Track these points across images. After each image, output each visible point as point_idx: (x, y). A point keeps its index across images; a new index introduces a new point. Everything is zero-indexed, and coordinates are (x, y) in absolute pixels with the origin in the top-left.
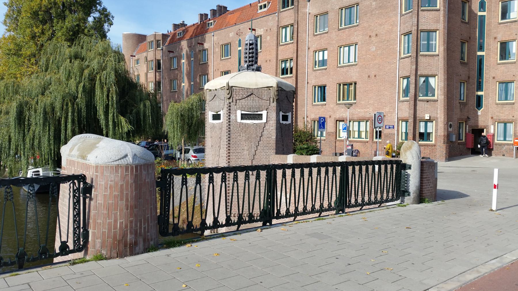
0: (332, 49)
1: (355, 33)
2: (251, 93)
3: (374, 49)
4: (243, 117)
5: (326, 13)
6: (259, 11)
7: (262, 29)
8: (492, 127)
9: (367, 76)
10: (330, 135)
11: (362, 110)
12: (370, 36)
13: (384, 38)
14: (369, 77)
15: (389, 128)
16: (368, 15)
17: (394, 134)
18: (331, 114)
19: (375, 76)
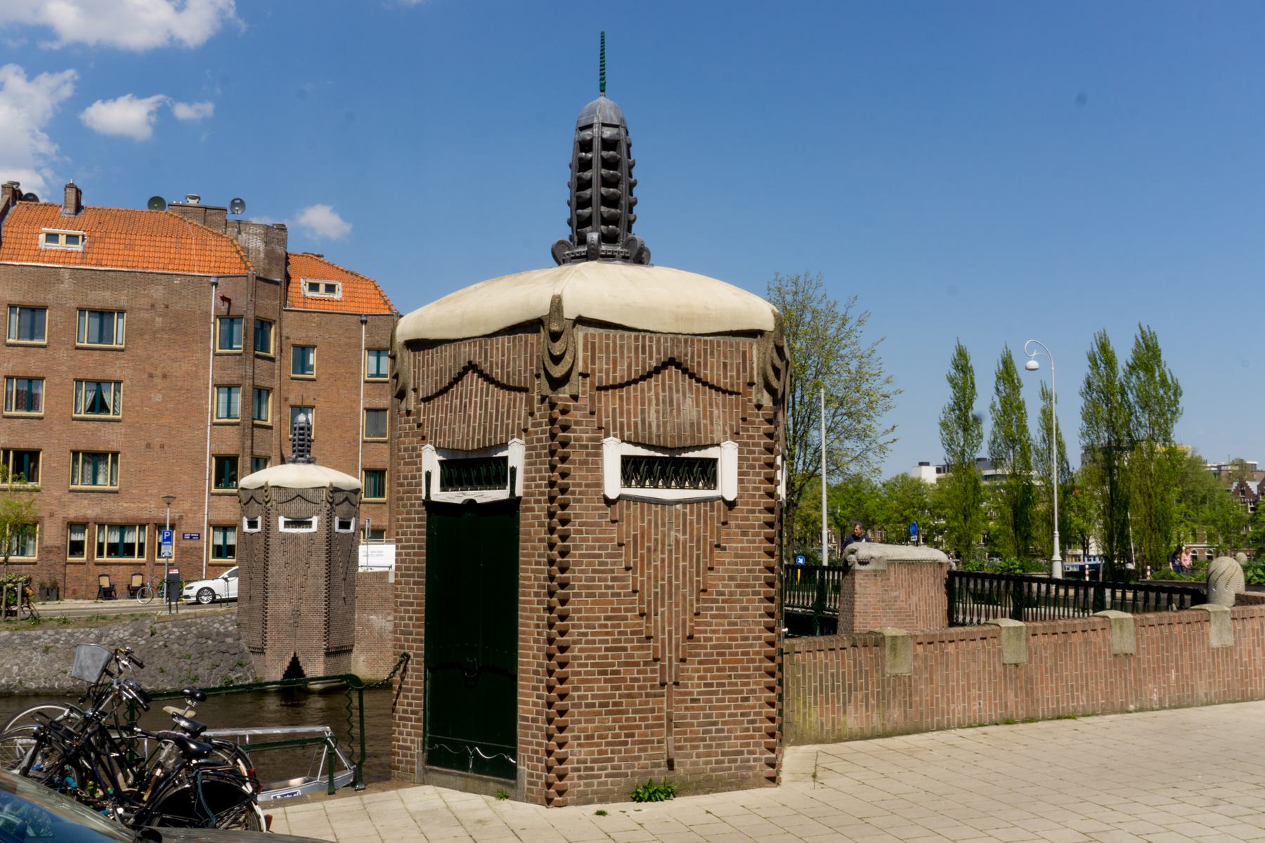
0: (57, 380)
1: (117, 362)
3: (158, 398)
5: (43, 309)
9: (144, 443)
10: (50, 552)
11: (132, 505)
13: (179, 384)
15: (191, 538)
16: (147, 337)
17: (202, 549)
18: (54, 508)
19: (162, 447)
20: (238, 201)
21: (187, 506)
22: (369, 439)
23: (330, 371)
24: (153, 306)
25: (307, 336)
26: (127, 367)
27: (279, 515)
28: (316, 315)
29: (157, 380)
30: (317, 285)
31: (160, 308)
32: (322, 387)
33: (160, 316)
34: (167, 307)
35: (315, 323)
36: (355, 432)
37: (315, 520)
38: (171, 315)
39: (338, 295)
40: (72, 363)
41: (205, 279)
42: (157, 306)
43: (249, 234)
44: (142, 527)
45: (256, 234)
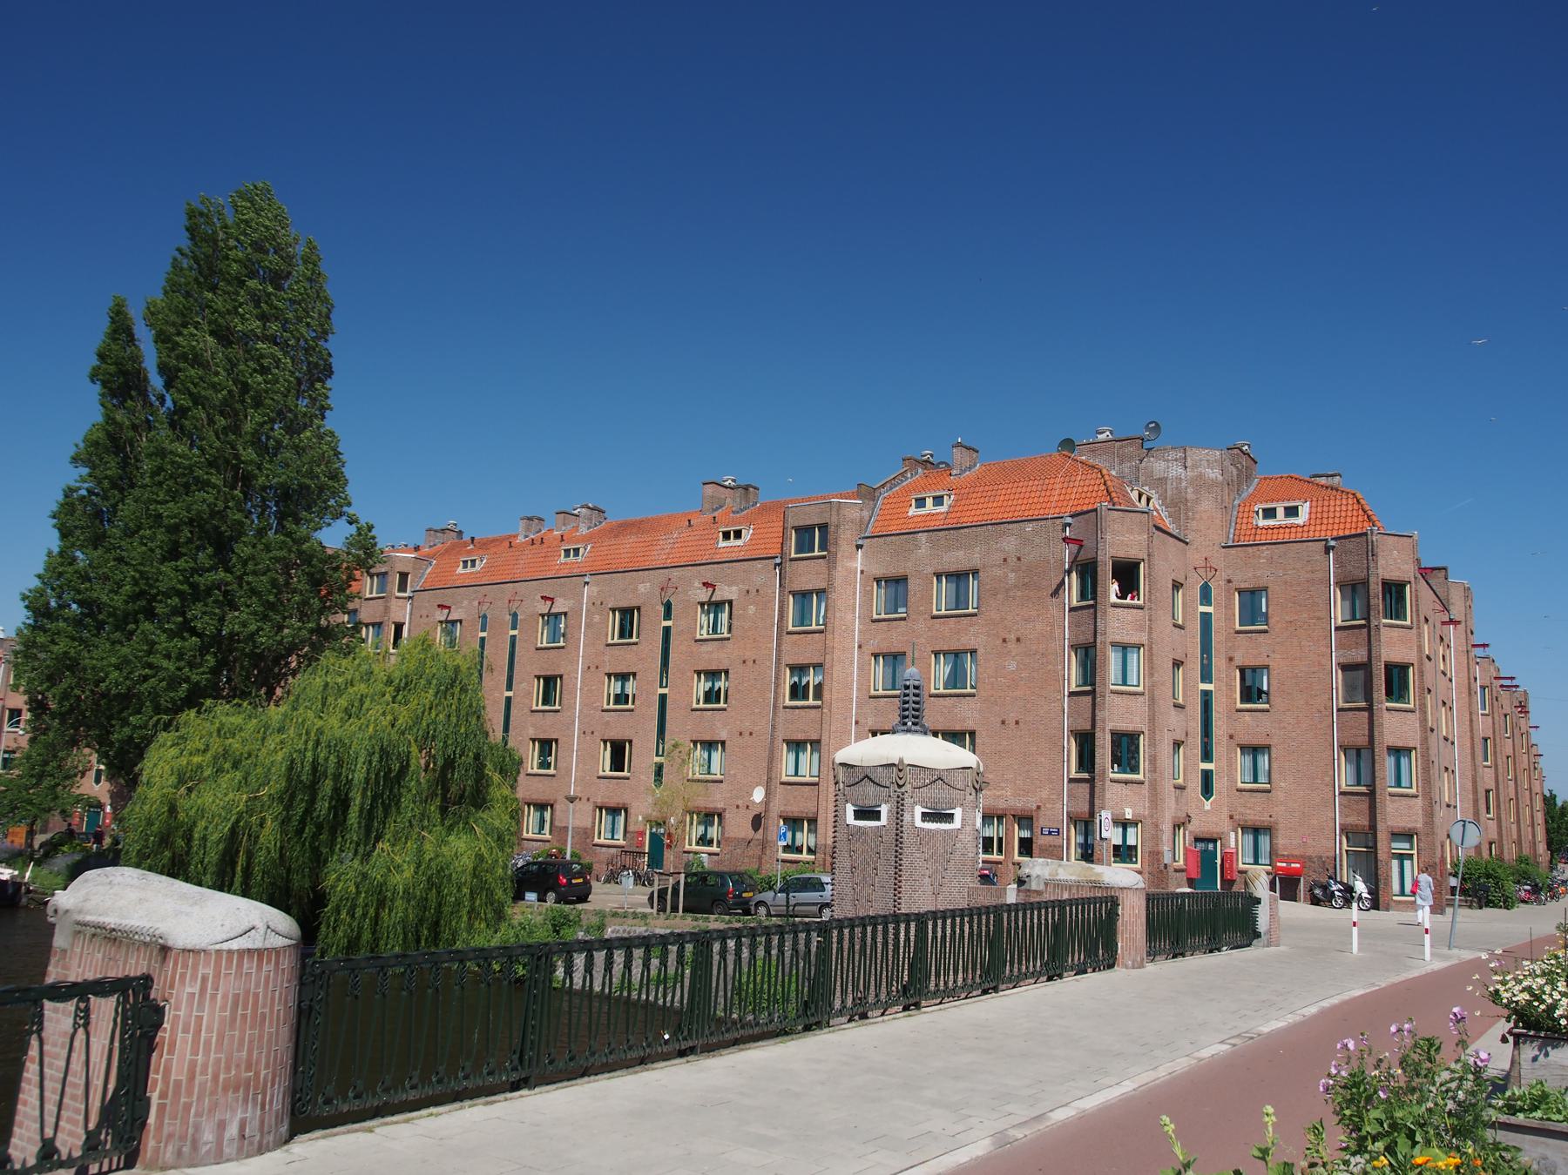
2: (939, 777)
3: (1012, 666)
4: (926, 817)
6: (722, 544)
7: (734, 588)
8: (1232, 835)
12: (1004, 640)
14: (1003, 722)
15: (1050, 833)
19: (1017, 723)
20: (1153, 425)
21: (1045, 794)
22: (1347, 705)
23: (1288, 618)
24: (1005, 560)
26: (981, 633)
27: (847, 801)
28: (1264, 548)
29: (1012, 646)
30: (1275, 509)
31: (1012, 561)
32: (1278, 640)
33: (1013, 571)
34: (1019, 559)
35: (1264, 558)
37: (884, 810)
38: (1024, 568)
39: (1302, 518)
40: (930, 633)
41: (1058, 521)
42: (1009, 560)
43: (1168, 461)
44: (1000, 818)
45: (1176, 460)
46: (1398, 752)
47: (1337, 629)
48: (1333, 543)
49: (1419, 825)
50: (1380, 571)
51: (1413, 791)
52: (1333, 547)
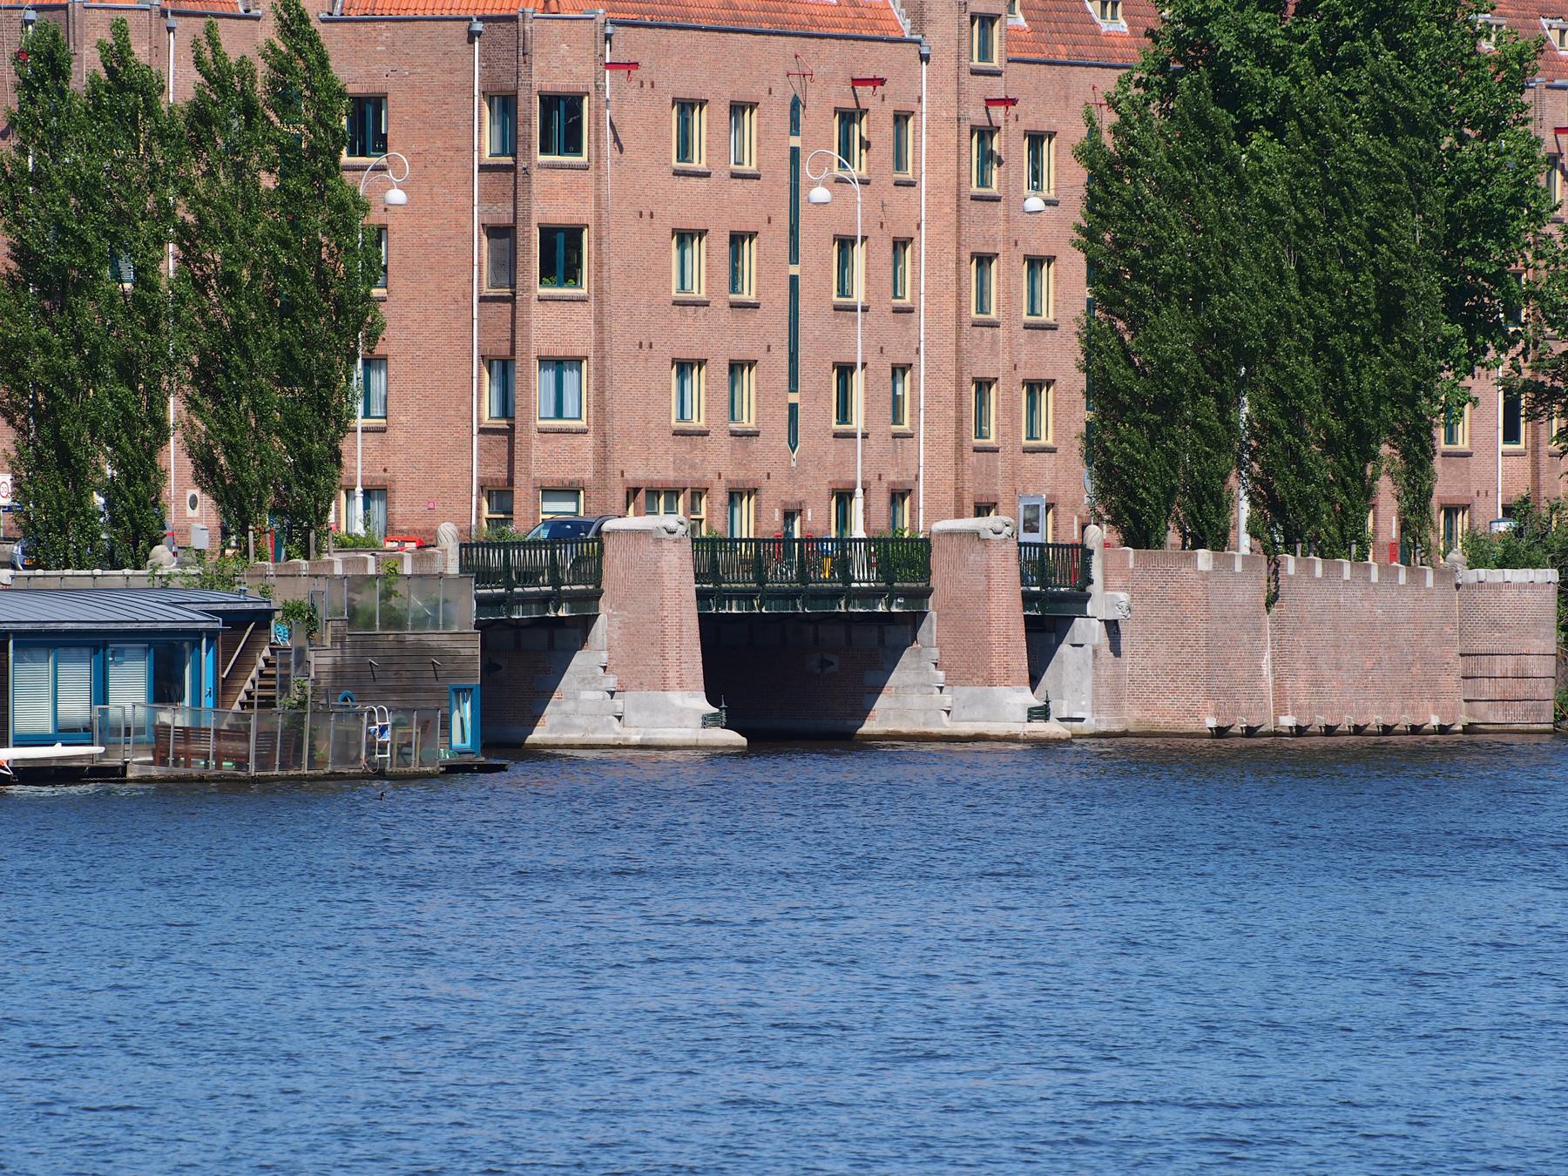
22: (493, 292)
25: (368, 74)
28: (383, 26)
35: (382, 43)
36: (466, 277)
46: (558, 364)
47: (482, 168)
48: (478, 26)
49: (588, 476)
50: (535, 79)
51: (582, 424)
52: (479, 34)
